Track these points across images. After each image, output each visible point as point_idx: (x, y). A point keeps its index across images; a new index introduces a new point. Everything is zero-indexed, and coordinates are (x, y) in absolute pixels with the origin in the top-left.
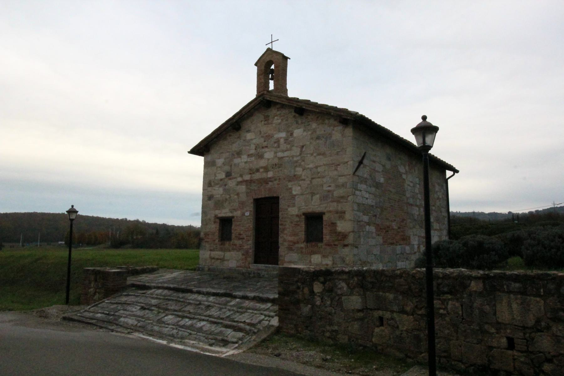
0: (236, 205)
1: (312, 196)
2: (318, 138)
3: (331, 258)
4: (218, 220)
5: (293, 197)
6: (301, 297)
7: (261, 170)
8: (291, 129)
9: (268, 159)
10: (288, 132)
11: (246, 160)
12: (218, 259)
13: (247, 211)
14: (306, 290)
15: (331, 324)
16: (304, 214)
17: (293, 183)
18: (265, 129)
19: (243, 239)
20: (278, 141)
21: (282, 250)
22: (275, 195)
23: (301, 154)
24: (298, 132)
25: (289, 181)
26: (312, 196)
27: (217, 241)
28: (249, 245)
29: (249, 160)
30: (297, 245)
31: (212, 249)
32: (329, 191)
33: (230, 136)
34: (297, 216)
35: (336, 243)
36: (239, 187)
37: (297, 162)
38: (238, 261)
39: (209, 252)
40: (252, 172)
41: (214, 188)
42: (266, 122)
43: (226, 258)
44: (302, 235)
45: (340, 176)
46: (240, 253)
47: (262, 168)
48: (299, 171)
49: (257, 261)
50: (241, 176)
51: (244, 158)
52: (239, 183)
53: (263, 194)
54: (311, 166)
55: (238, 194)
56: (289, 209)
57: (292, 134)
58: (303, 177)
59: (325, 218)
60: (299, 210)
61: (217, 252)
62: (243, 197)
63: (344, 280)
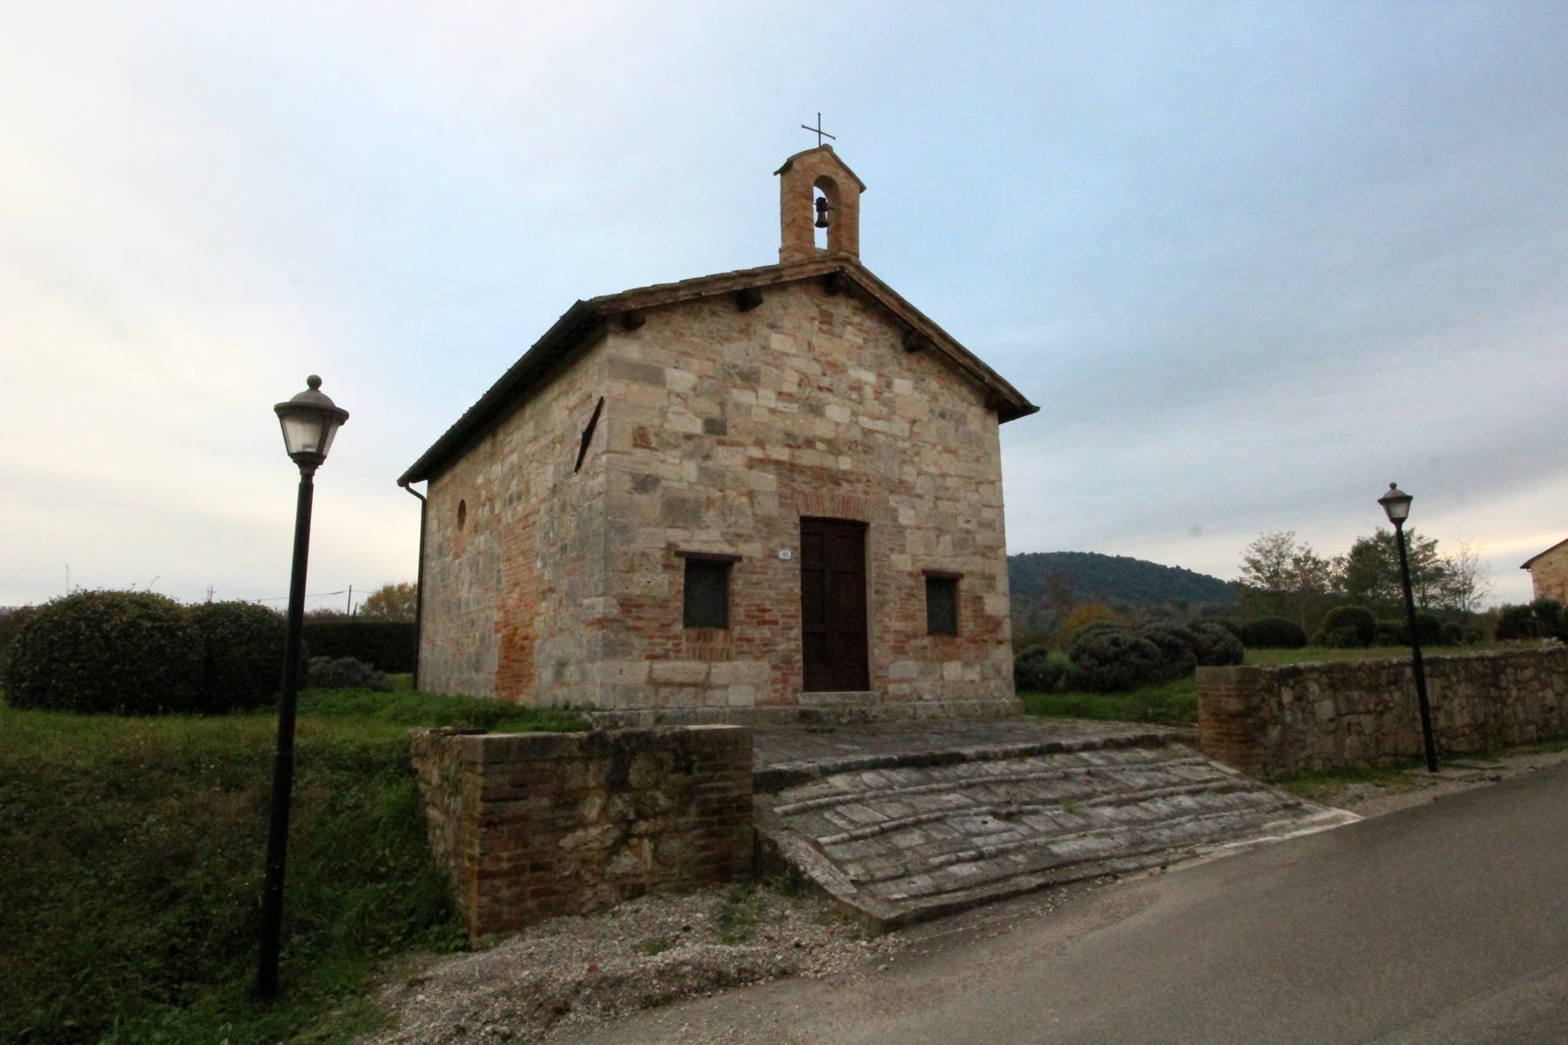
0: (746, 524)
1: (938, 536)
2: (943, 416)
3: (978, 668)
4: (681, 563)
5: (901, 530)
6: (1267, 716)
7: (820, 446)
8: (886, 371)
9: (838, 424)
10: (880, 375)
11: (772, 405)
12: (682, 685)
13: (783, 546)
14: (1273, 703)
15: (1303, 749)
16: (925, 572)
17: (897, 498)
18: (821, 342)
19: (775, 623)
20: (857, 387)
21: (878, 652)
22: (859, 518)
23: (910, 438)
24: (903, 386)
25: (891, 492)
26: (938, 536)
27: (679, 627)
28: (791, 641)
29: (781, 406)
30: (913, 642)
31: (658, 651)
32: (968, 532)
33: (713, 313)
34: (910, 574)
35: (986, 637)
36: (755, 473)
37: (904, 451)
38: (757, 687)
39: (647, 663)
40: (791, 441)
41: (661, 455)
42: (825, 327)
43: (714, 680)
44: (922, 622)
45: (985, 505)
46: (765, 665)
47: (822, 440)
48: (909, 473)
49: (811, 683)
50: (760, 444)
51: (767, 397)
52: (752, 463)
53: (827, 509)
54: (933, 470)
55: (751, 494)
56: (894, 557)
57: (889, 385)
58: (918, 491)
59: (964, 585)
60: (914, 559)
61: (679, 664)
62: (769, 506)
63: (1316, 680)
